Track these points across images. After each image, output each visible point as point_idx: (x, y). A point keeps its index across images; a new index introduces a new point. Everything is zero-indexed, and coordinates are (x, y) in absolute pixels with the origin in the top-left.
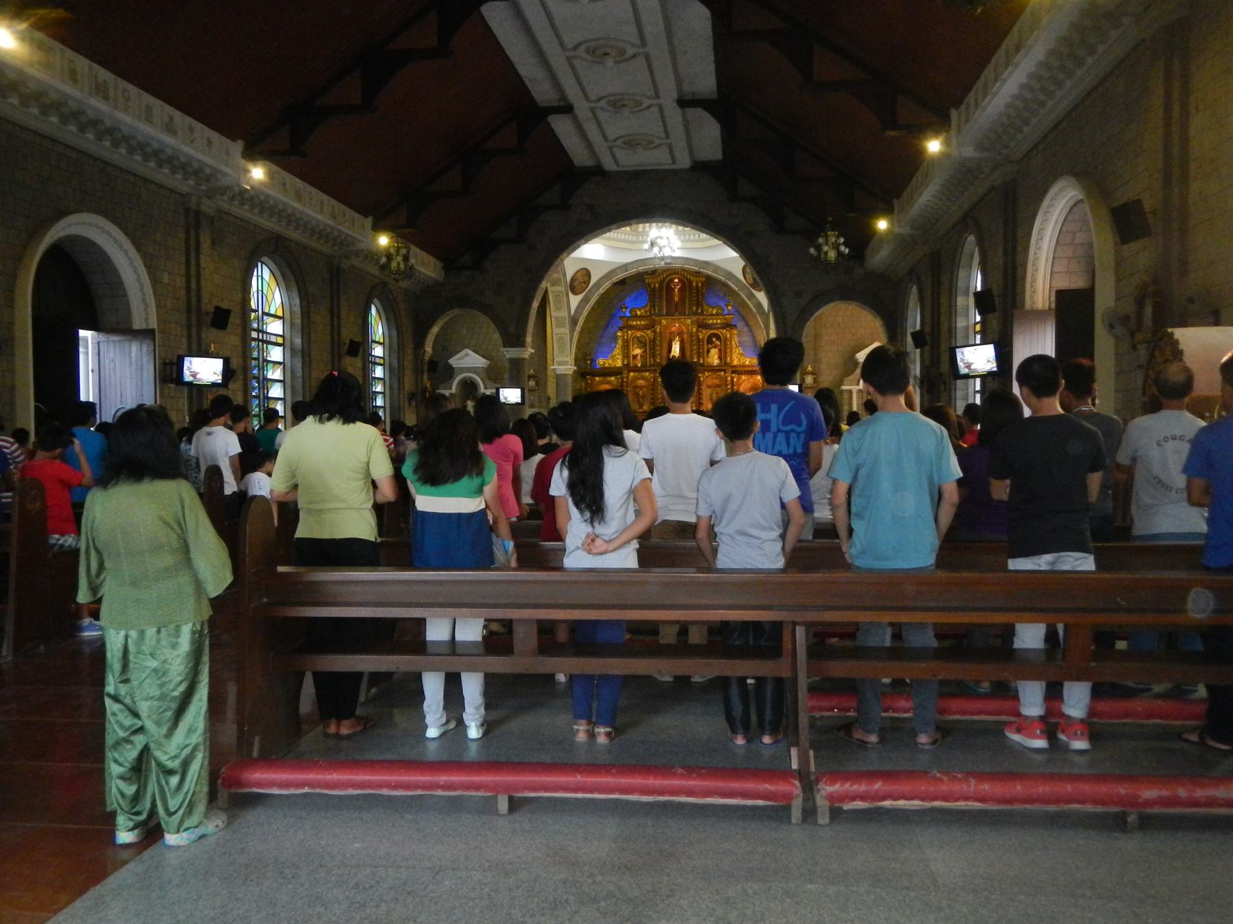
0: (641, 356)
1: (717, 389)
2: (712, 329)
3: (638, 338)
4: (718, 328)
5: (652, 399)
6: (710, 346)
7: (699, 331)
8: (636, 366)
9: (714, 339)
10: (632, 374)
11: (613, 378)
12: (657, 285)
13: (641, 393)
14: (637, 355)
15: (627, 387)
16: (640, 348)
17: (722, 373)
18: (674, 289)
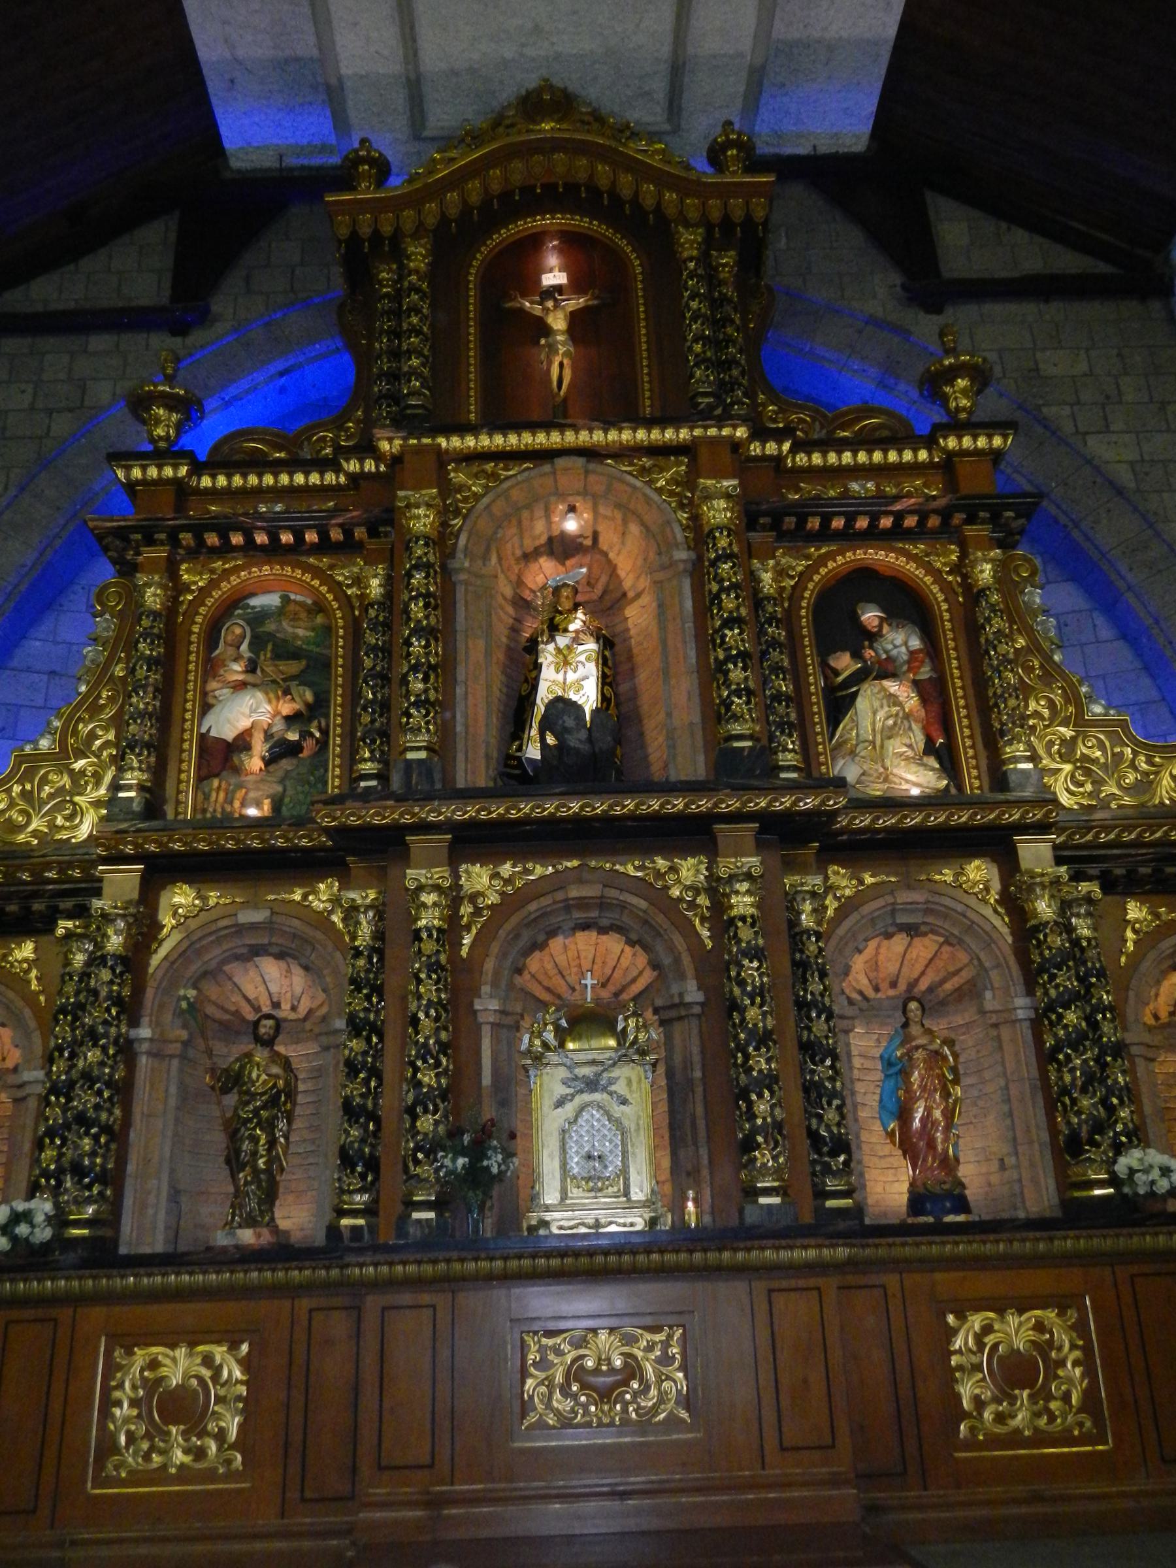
0: (281, 751)
1: (939, 1025)
2: (849, 537)
3: (257, 619)
4: (898, 533)
5: (350, 1111)
6: (845, 663)
7: (750, 551)
8: (229, 823)
9: (870, 616)
10: (182, 897)
11: (26, 950)
12: (418, 255)
13: (260, 1077)
14: (242, 743)
15: (130, 1010)
16: (281, 688)
17: (979, 871)
18: (547, 331)
